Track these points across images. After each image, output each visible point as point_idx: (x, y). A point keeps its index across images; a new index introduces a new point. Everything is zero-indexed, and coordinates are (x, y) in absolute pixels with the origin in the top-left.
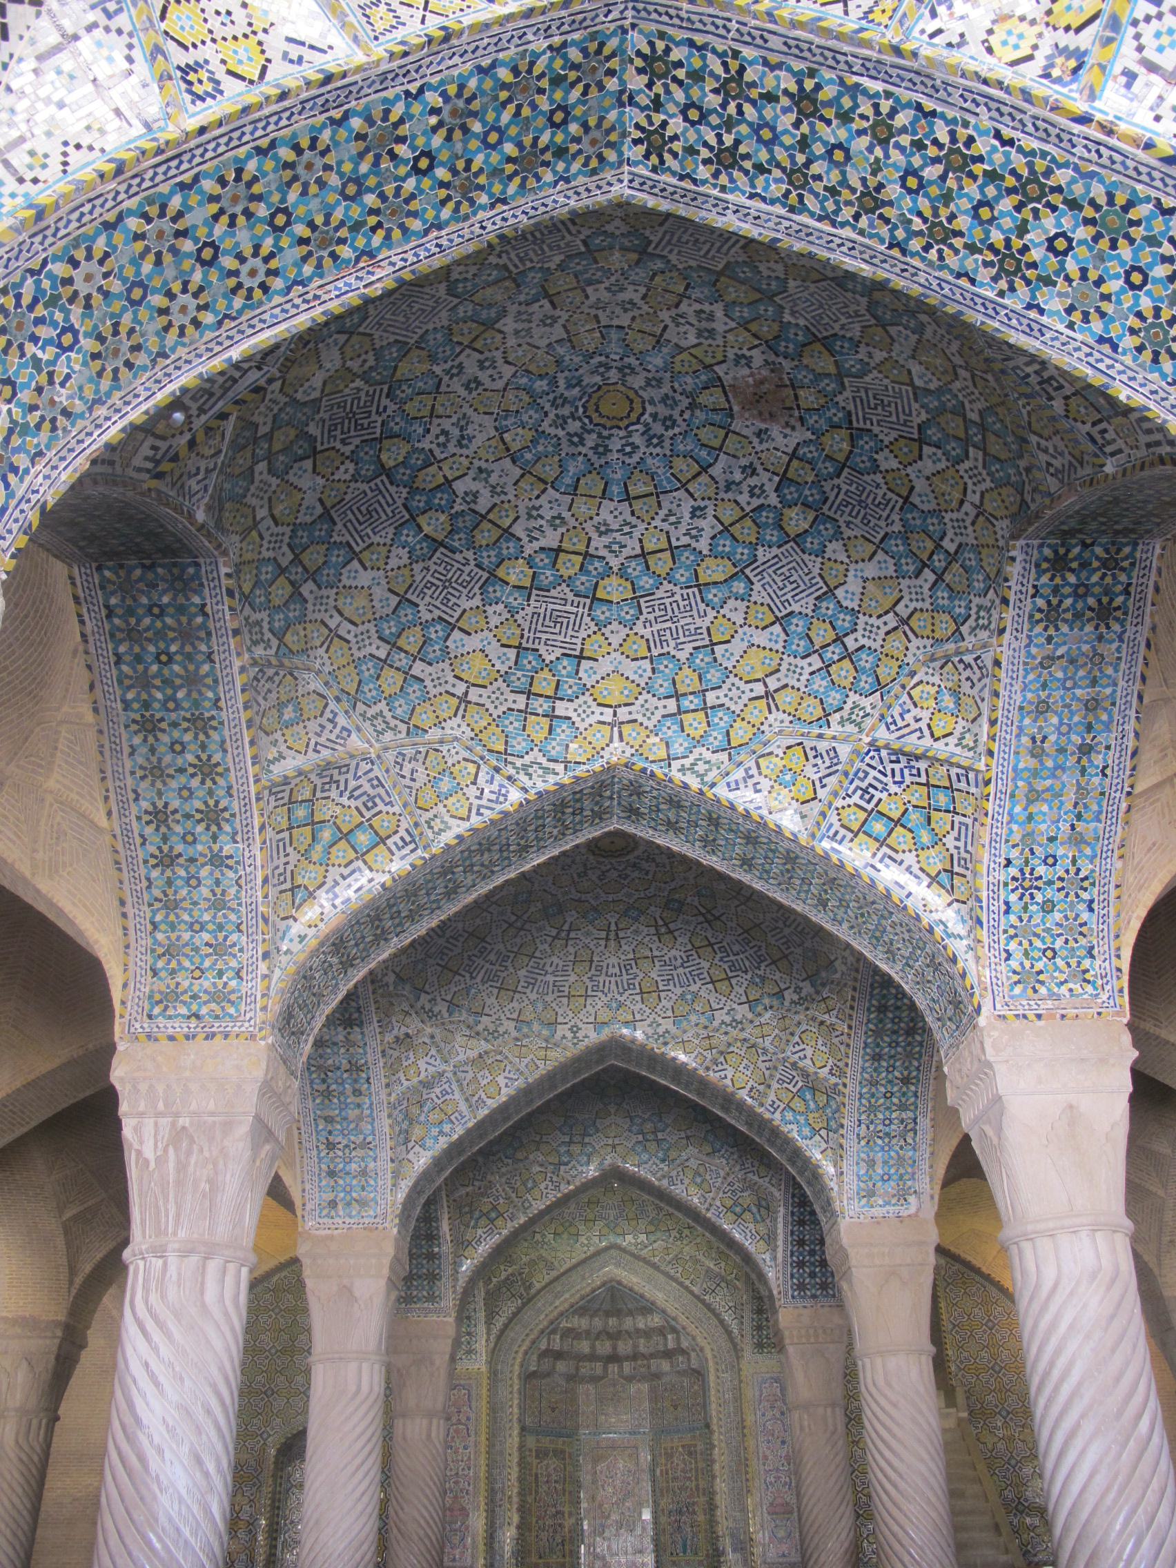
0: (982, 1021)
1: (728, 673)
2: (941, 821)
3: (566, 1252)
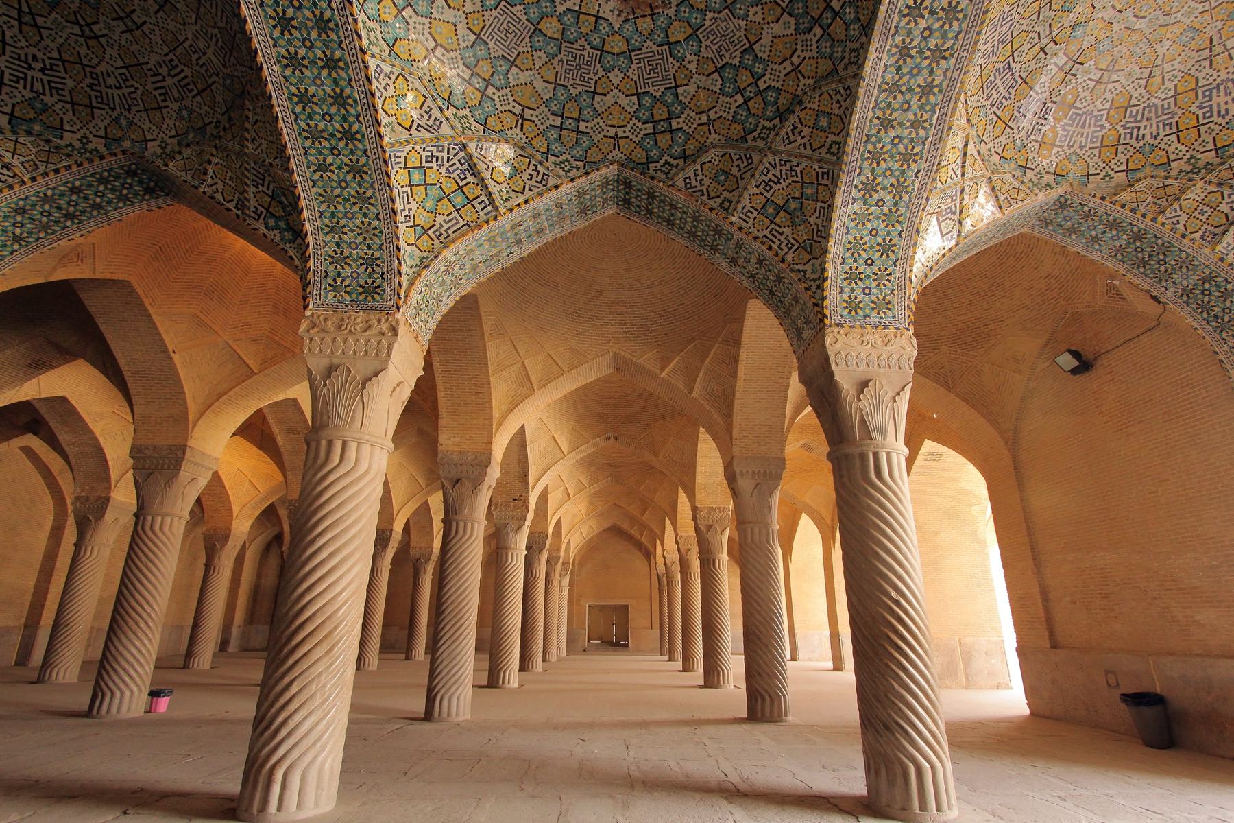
2: (445, 206)
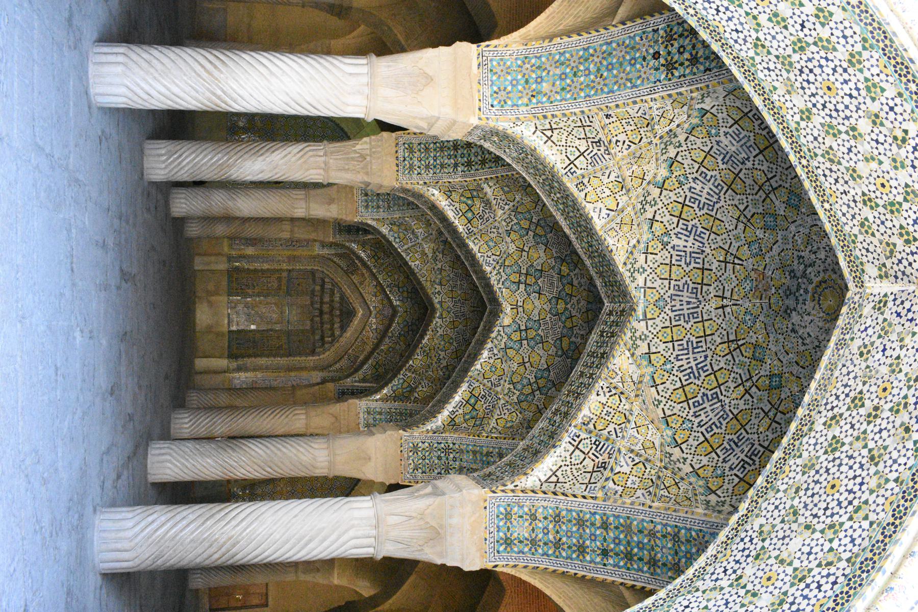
0: (401, 431)
1: (533, 348)
3: (368, 290)
